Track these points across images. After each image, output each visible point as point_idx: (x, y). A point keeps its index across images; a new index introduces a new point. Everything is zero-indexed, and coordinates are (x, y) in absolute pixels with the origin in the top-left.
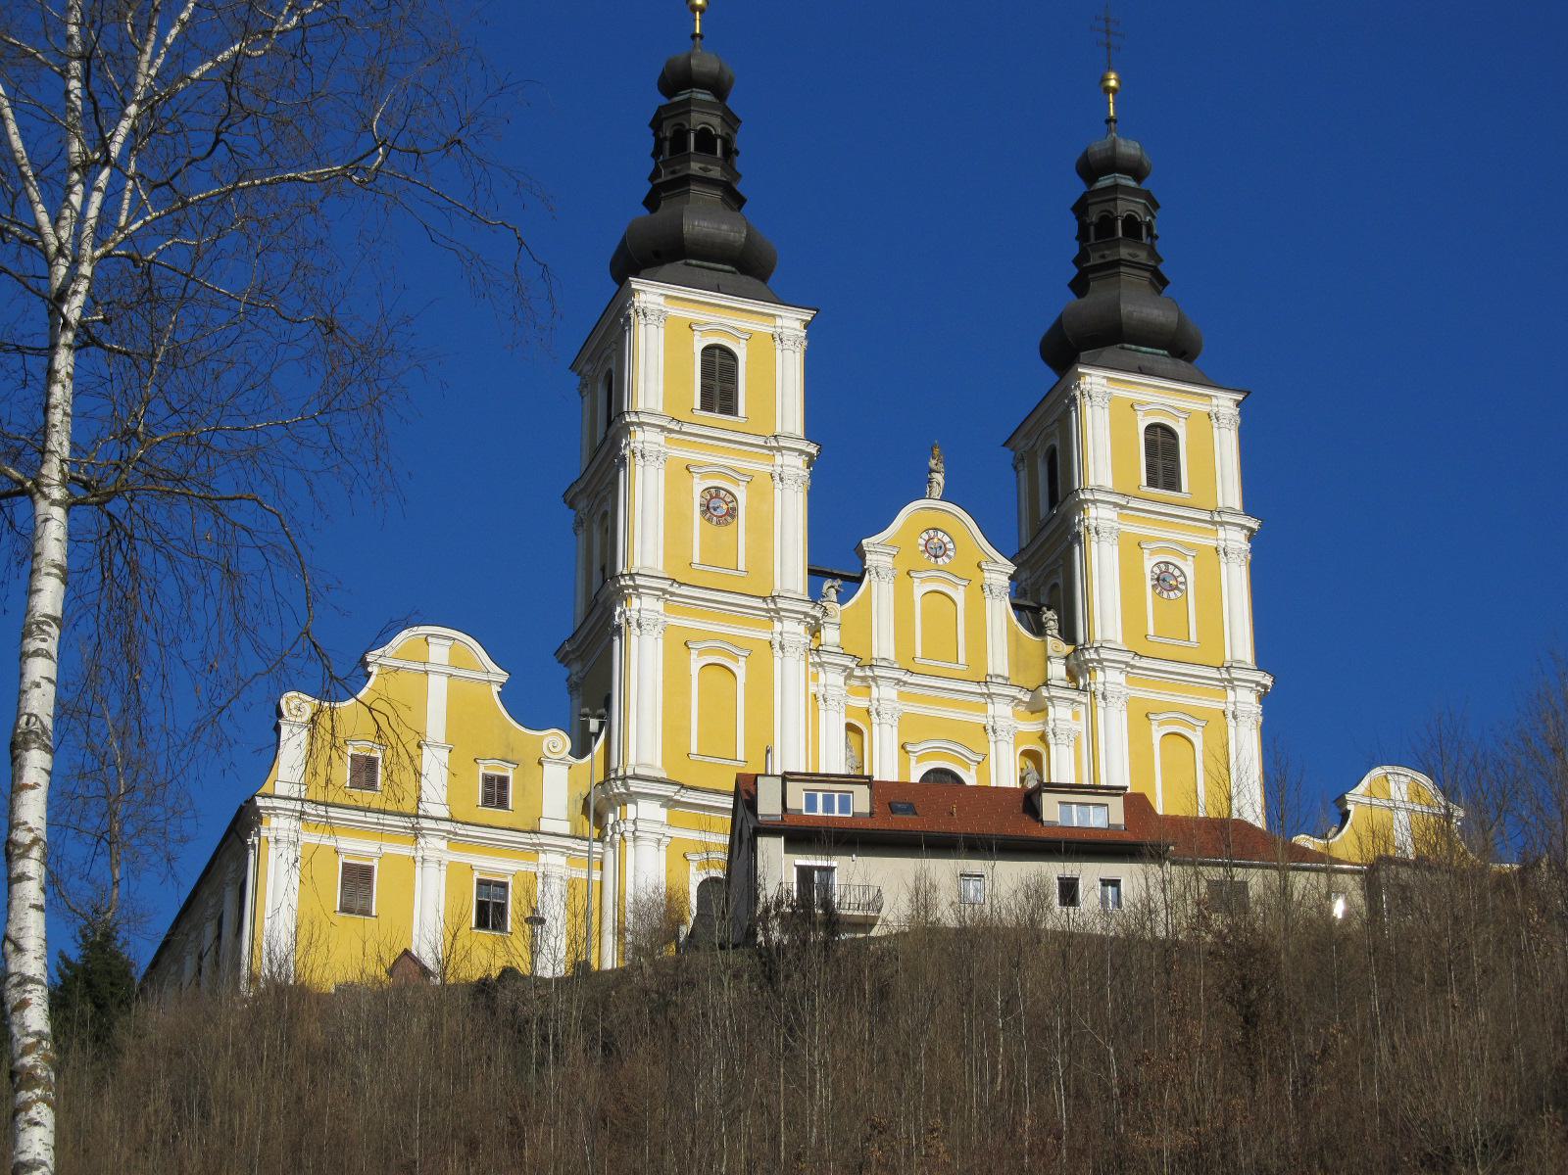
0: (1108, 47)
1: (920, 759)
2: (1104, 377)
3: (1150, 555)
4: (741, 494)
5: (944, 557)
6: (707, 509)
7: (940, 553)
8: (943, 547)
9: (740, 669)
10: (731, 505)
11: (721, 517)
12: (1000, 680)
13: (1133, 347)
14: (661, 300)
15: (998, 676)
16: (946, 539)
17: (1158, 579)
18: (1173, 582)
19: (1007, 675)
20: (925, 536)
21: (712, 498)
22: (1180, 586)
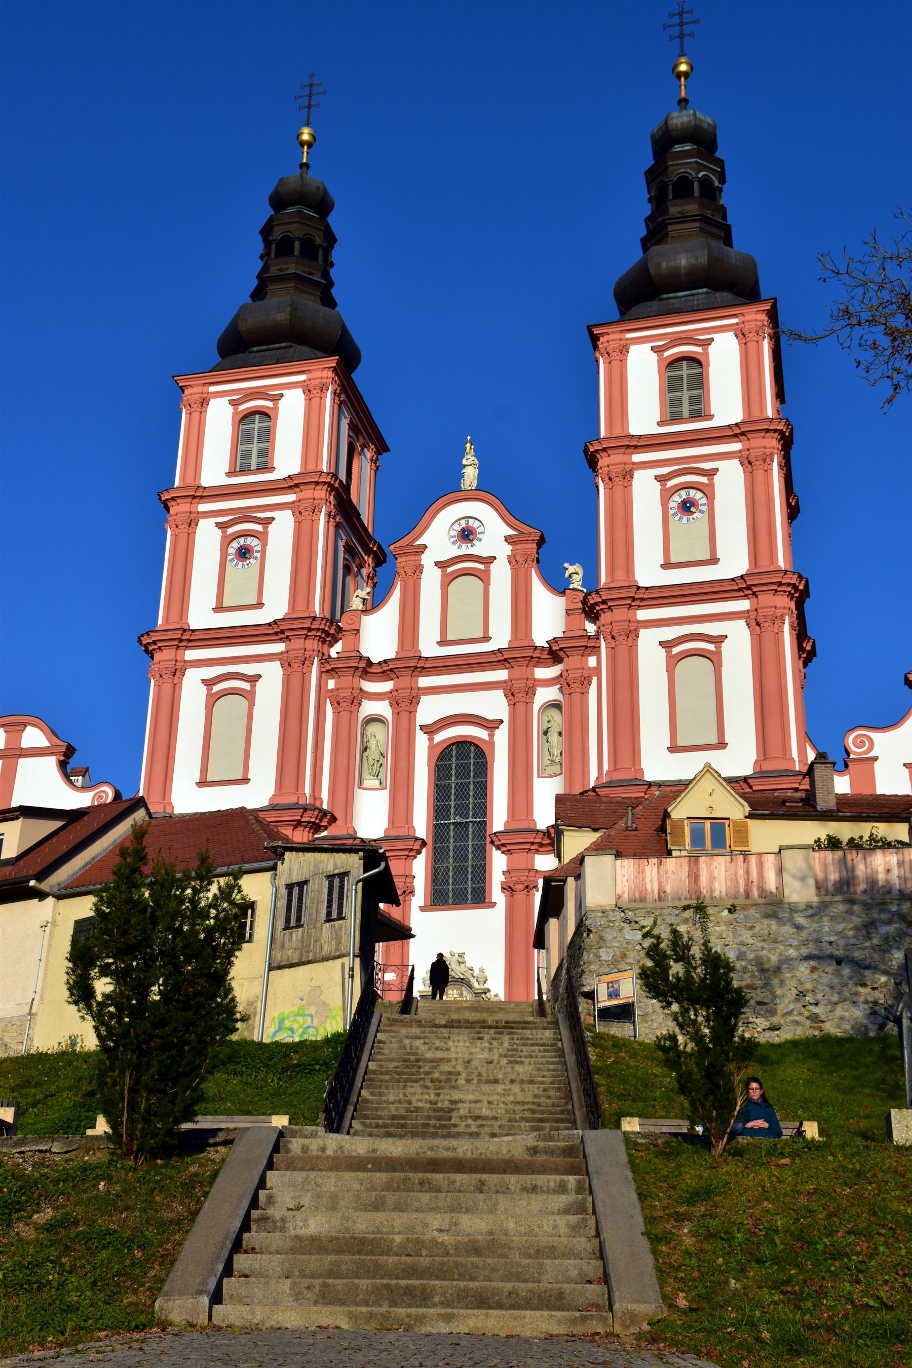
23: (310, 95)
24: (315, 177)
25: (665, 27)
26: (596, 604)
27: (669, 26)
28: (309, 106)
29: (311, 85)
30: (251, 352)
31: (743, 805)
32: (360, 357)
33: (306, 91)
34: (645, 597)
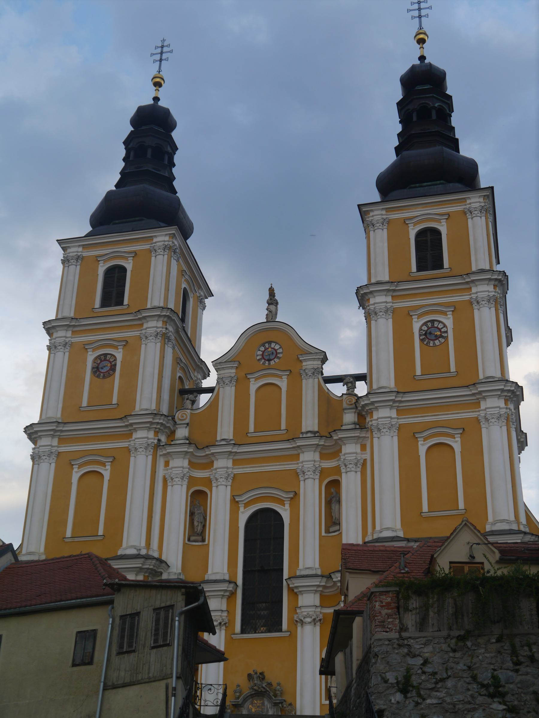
0: (420, 17)
1: (246, 505)
2: (383, 209)
3: (418, 318)
4: (119, 355)
5: (275, 360)
6: (96, 370)
8: (275, 353)
9: (107, 474)
10: (113, 363)
11: (106, 372)
12: (309, 435)
13: (417, 185)
14: (80, 249)
15: (307, 432)
16: (277, 347)
17: (425, 334)
18: (439, 333)
19: (316, 429)
20: (262, 349)
21: (101, 361)
22: (443, 335)
23: (162, 53)
25: (409, 11)
26: (366, 405)
27: (411, 10)
28: (161, 60)
29: (162, 47)
30: (114, 224)
31: (494, 552)
33: (159, 50)
34: (403, 399)
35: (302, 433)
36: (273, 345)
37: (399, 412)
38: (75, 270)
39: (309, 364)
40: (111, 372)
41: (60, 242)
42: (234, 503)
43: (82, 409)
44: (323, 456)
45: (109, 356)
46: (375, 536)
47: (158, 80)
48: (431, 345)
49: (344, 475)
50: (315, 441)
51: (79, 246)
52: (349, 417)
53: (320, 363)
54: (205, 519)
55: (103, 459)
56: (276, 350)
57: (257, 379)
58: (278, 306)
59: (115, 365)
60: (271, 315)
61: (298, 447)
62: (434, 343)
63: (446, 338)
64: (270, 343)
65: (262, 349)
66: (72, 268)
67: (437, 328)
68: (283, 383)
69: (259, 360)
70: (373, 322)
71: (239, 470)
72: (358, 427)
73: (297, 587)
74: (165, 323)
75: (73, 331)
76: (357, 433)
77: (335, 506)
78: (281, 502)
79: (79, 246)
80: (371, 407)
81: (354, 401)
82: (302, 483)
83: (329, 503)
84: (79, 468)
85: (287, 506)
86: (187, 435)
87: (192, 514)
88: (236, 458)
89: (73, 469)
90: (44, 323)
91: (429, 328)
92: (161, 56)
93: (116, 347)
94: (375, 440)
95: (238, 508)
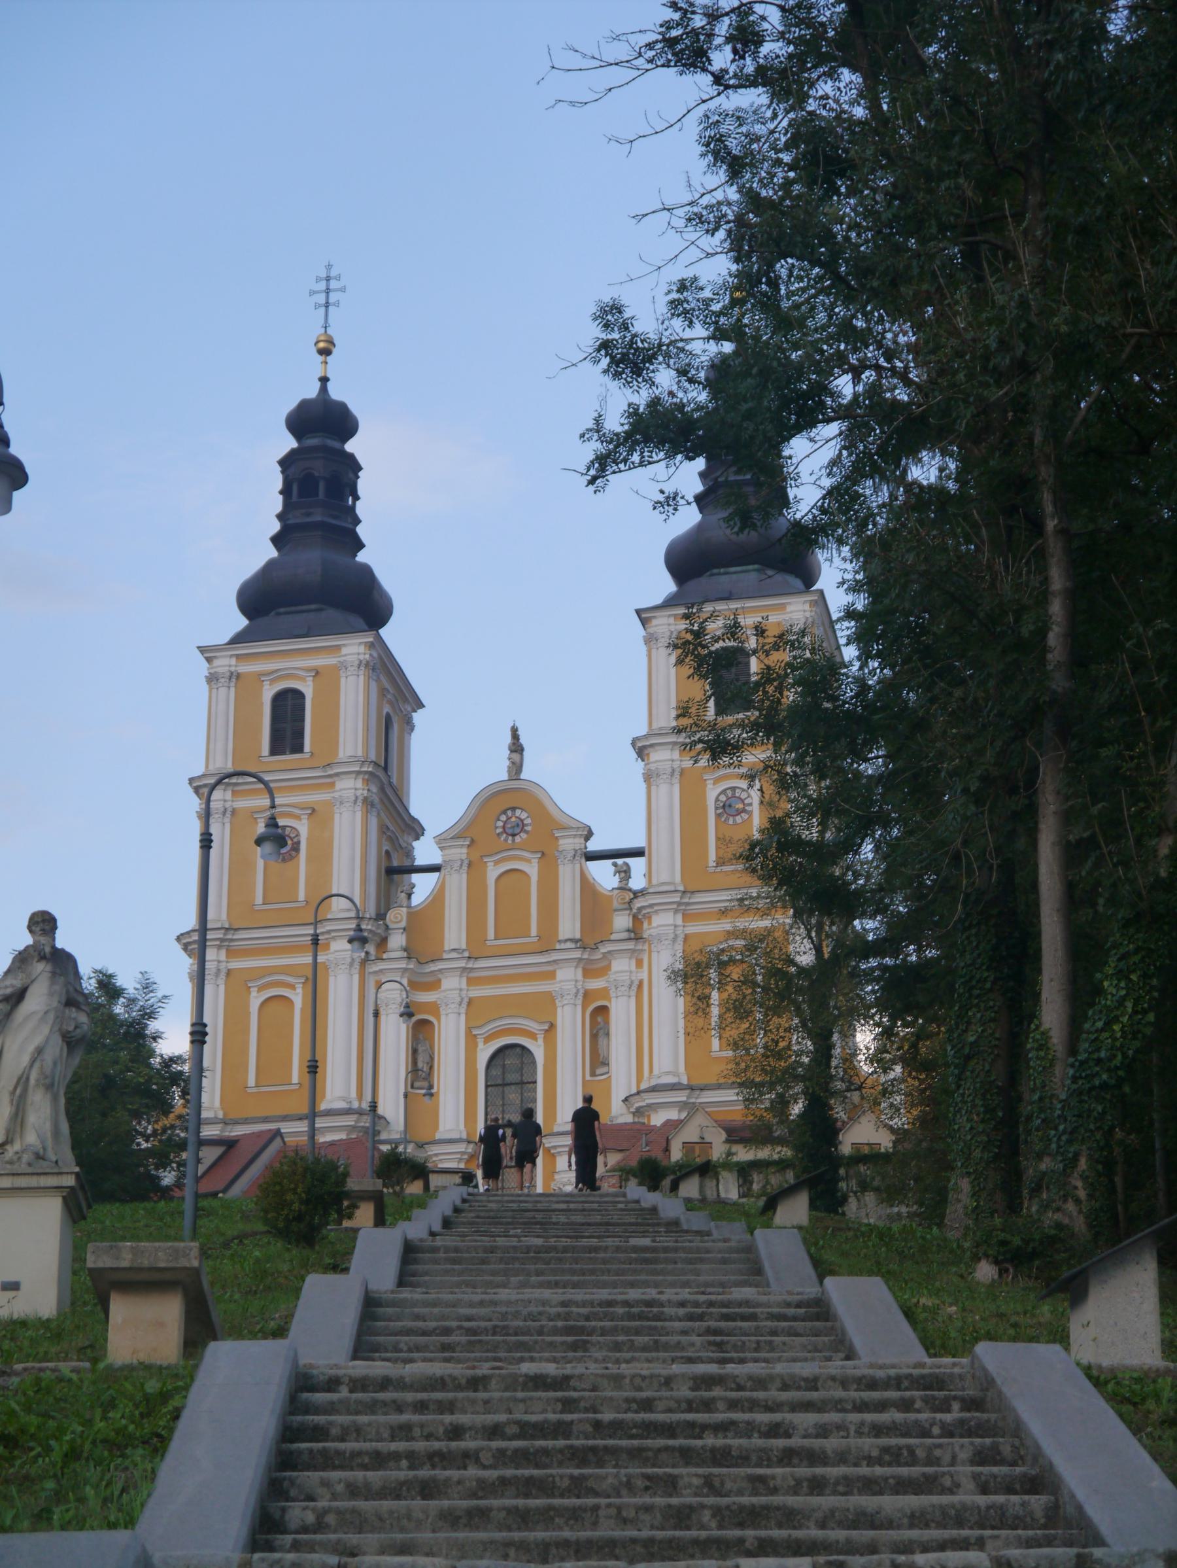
1: (487, 1040)
2: (669, 616)
7: (517, 830)
8: (521, 825)
13: (722, 570)
14: (233, 661)
15: (566, 941)
16: (524, 815)
17: (724, 807)
18: (740, 806)
19: (578, 936)
20: (503, 818)
23: (328, 291)
24: (336, 393)
28: (327, 305)
29: (328, 279)
30: (279, 614)
32: (391, 614)
33: (322, 286)
35: (559, 941)
36: (518, 812)
37: (687, 917)
38: (227, 695)
39: (569, 844)
40: (293, 853)
41: (202, 650)
42: (471, 1039)
43: (256, 908)
44: (588, 973)
45: (288, 829)
46: (653, 1083)
47: (322, 345)
48: (731, 822)
49: (613, 1000)
50: (577, 954)
51: (231, 656)
52: (622, 921)
53: (582, 840)
54: (432, 1059)
55: (291, 980)
56: (522, 821)
57: (497, 863)
58: (525, 753)
59: (298, 843)
60: (516, 768)
61: (555, 961)
62: (734, 820)
63: (750, 813)
64: (513, 809)
65: (503, 818)
66: (223, 691)
67: (739, 798)
68: (532, 870)
69: (498, 834)
70: (653, 788)
71: (477, 992)
72: (632, 935)
73: (555, 1147)
74: (366, 781)
75: (233, 791)
76: (630, 945)
77: (602, 1041)
78: (533, 1036)
79: (231, 656)
80: (649, 910)
81: (627, 900)
82: (559, 1010)
83: (594, 1037)
84: (258, 991)
85: (541, 1041)
86: (404, 944)
87: (415, 1052)
88: (471, 975)
89: (250, 993)
90: (191, 780)
91: (728, 799)
92: (327, 297)
93: (298, 818)
94: (654, 955)
95: (476, 1046)
